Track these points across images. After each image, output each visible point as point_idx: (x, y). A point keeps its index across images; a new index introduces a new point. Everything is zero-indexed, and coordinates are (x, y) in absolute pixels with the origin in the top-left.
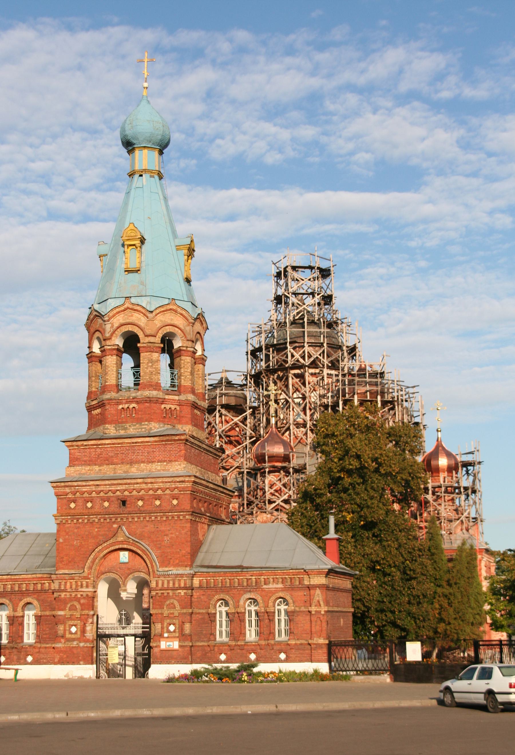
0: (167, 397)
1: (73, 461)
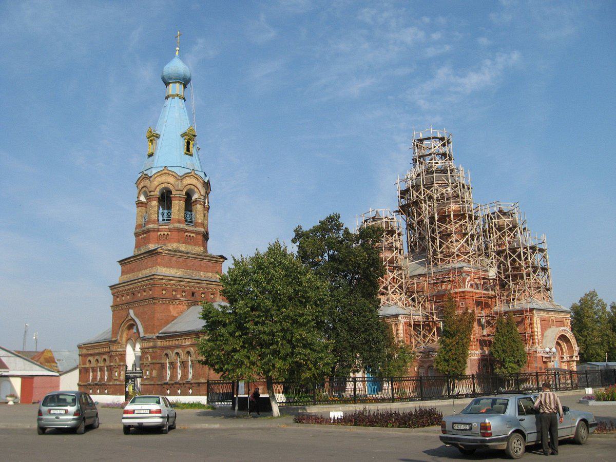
0: (160, 227)
1: (123, 273)
